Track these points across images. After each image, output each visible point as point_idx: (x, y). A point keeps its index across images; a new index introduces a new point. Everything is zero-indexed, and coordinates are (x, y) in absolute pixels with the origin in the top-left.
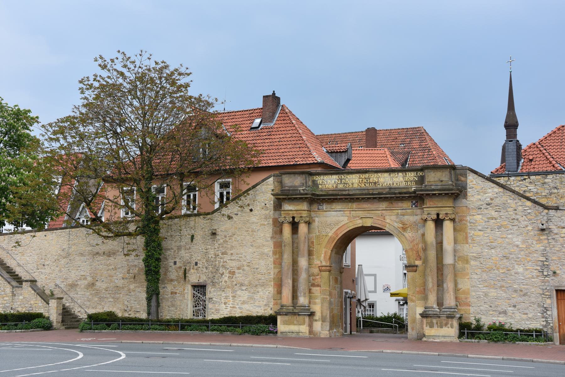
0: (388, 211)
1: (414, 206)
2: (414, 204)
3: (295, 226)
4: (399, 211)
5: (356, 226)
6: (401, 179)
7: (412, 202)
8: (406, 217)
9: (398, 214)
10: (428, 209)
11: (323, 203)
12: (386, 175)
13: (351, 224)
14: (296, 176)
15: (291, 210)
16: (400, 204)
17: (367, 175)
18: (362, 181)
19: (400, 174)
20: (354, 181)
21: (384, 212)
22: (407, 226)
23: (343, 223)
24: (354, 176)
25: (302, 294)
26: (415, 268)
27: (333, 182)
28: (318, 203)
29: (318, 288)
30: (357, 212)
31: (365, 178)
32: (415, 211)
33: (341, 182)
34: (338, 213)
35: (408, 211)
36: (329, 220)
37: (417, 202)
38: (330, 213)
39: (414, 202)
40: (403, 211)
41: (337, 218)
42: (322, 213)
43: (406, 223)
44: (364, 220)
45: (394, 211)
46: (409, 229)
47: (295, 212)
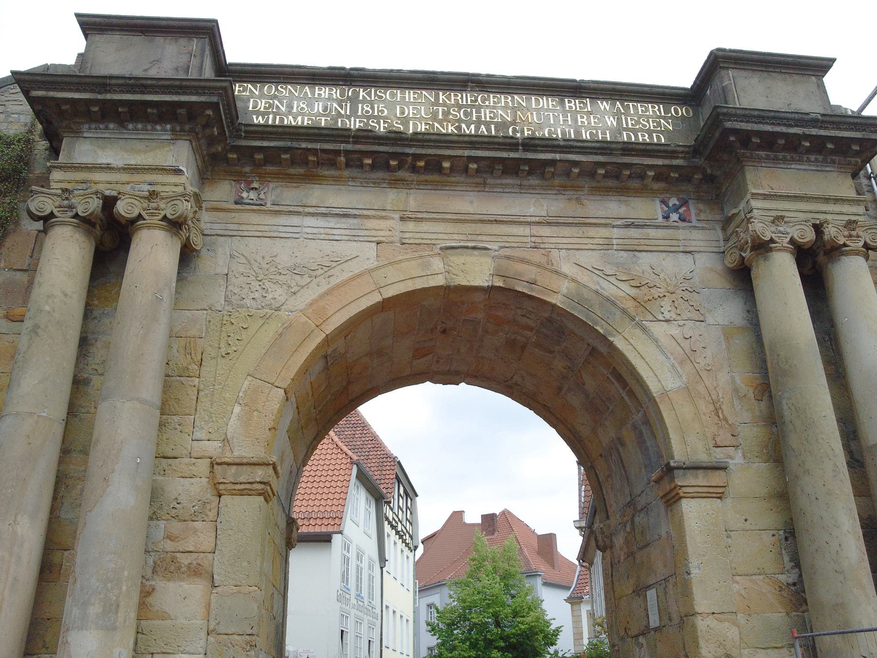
0: (566, 231)
1: (674, 217)
2: (676, 209)
3: (111, 239)
4: (616, 233)
5: (419, 284)
6: (611, 121)
7: (663, 202)
8: (646, 260)
9: (608, 245)
10: (767, 204)
11: (263, 178)
12: (548, 103)
13: (392, 274)
14: (159, 40)
15: (108, 168)
16: (613, 207)
17: (466, 98)
18: (446, 114)
19: (604, 105)
20: (410, 111)
21: (546, 231)
22: (655, 292)
23: (356, 268)
24: (410, 95)
25: (94, 610)
26: (716, 478)
27: (318, 107)
28: (239, 177)
29: (195, 589)
30: (425, 226)
31: (460, 107)
32: (681, 234)
33: (354, 111)
34: (332, 222)
35: (652, 233)
36: (285, 253)
37: (684, 203)
38: (295, 220)
39: (673, 201)
40: (633, 232)
41: (327, 247)
42: (255, 218)
43: (650, 278)
44: (457, 260)
45: (592, 232)
46: (666, 304)
47: (124, 177)
